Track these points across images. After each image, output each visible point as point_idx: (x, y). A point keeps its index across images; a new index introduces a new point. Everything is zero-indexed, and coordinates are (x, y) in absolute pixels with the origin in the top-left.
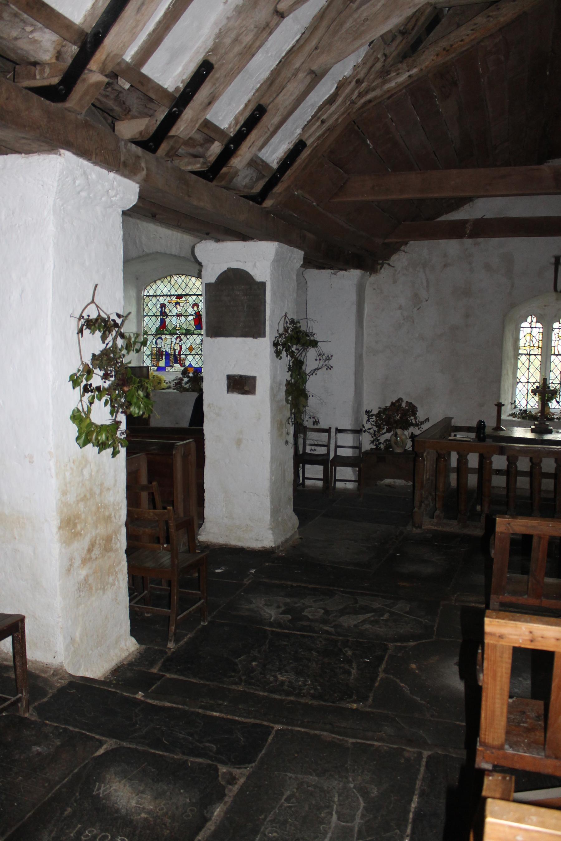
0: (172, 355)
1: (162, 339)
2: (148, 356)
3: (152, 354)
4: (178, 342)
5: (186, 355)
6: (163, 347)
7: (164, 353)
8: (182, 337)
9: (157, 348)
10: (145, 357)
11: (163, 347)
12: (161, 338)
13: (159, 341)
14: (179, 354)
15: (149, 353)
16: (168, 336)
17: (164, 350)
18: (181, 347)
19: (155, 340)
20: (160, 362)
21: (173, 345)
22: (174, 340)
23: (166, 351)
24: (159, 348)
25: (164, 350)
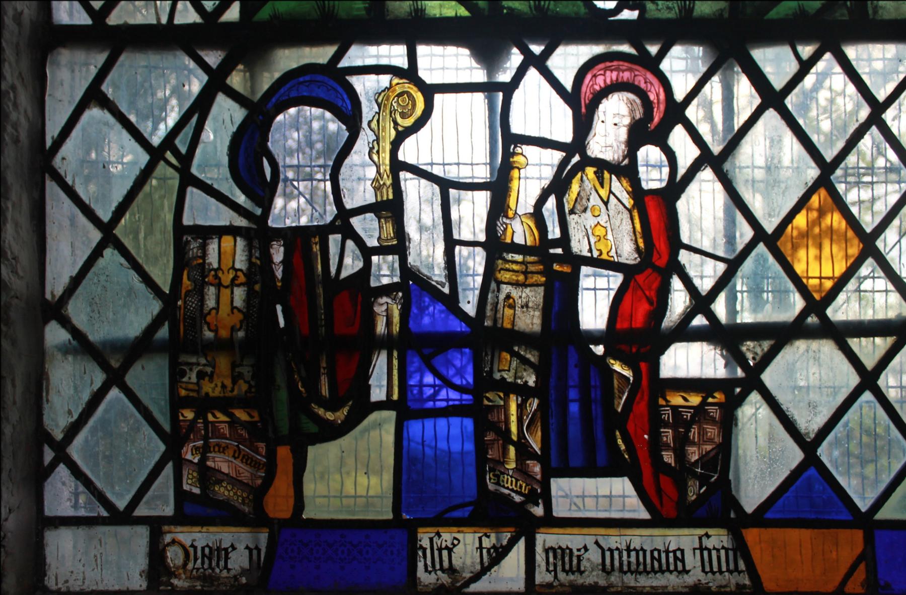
0: (510, 339)
1: (350, 116)
2: (114, 362)
3: (178, 331)
4: (608, 136)
5: (726, 337)
6: (368, 228)
7: (387, 314)
8: (682, 65)
9: (259, 234)
10: (69, 384)
11: (368, 228)
12: (331, 89)
13: (301, 130)
14: (640, 334)
15: (134, 317)
16: (443, 62)
17: (385, 271)
18: (657, 213)
19: (226, 115)
20: (321, 456)
21: (527, 188)
22: (539, 110)
23: (412, 281)
24: (300, 239)
25: (385, 271)
